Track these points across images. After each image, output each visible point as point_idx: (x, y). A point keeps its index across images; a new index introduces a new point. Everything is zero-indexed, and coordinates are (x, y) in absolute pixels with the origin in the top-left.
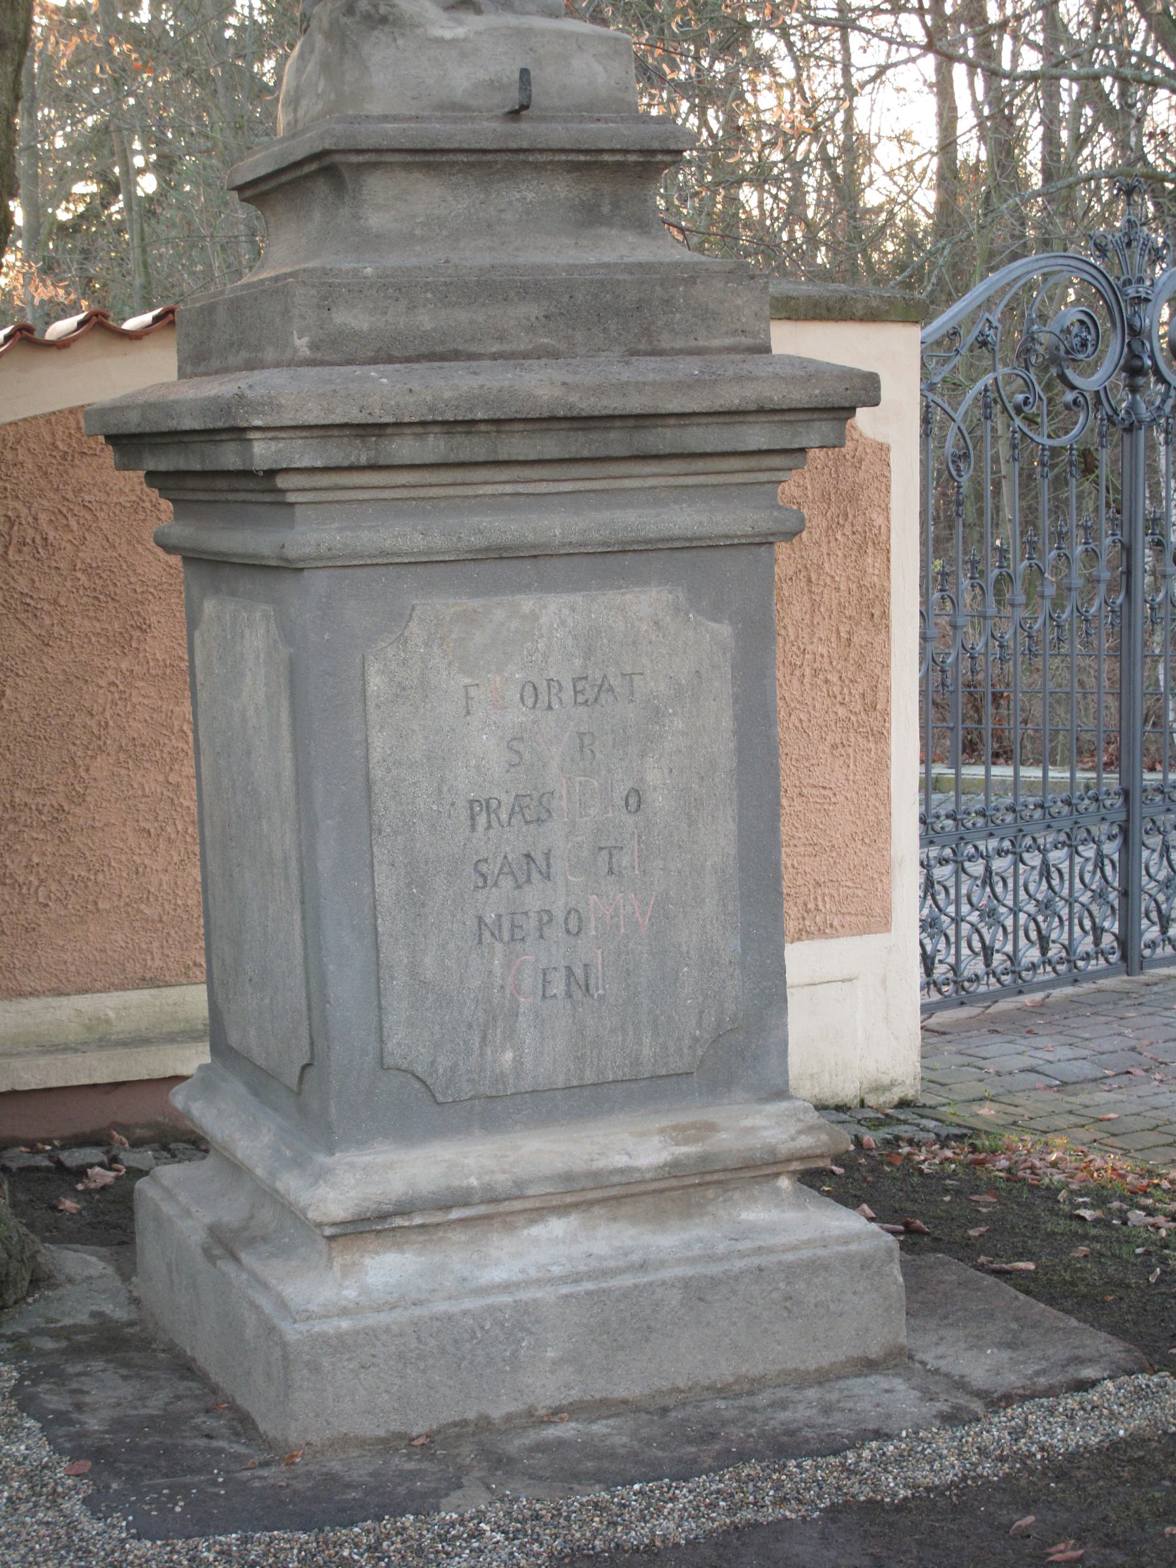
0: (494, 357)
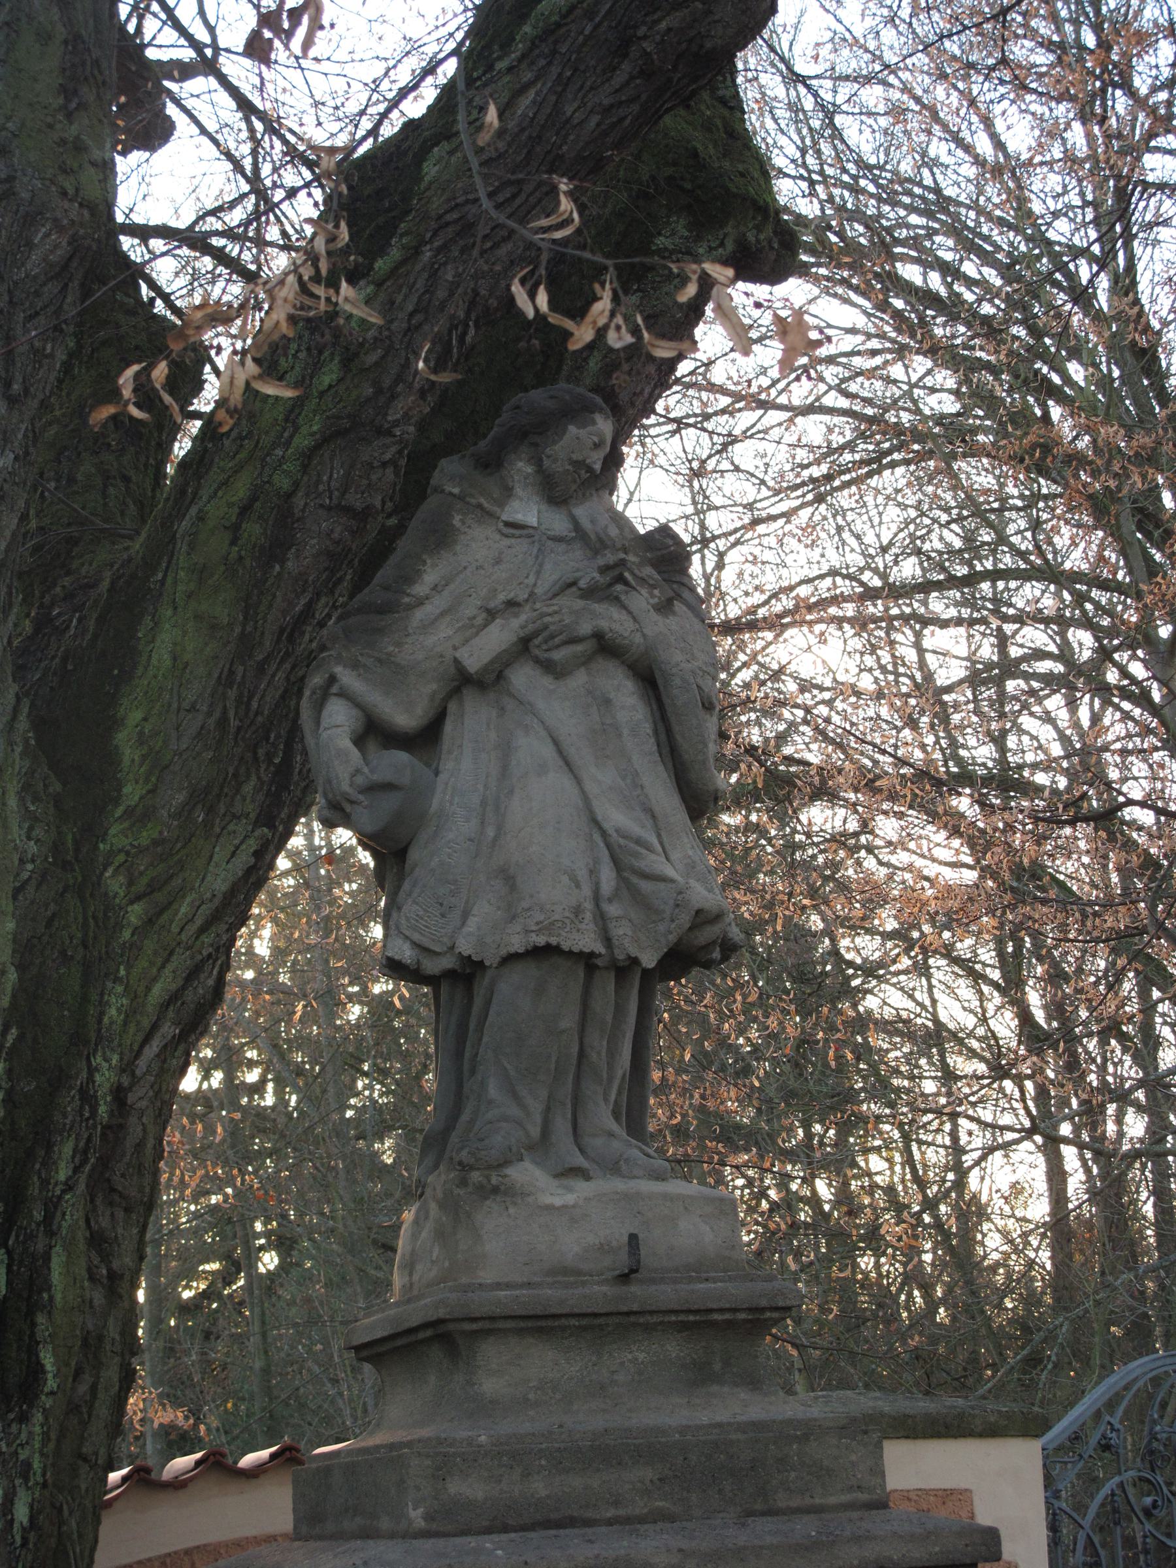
0: (610, 1522)
